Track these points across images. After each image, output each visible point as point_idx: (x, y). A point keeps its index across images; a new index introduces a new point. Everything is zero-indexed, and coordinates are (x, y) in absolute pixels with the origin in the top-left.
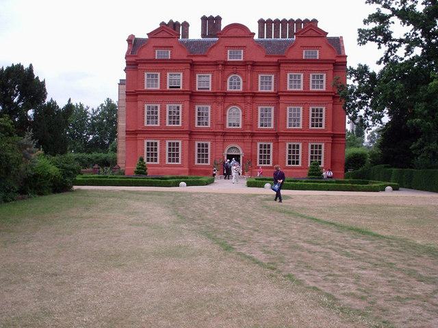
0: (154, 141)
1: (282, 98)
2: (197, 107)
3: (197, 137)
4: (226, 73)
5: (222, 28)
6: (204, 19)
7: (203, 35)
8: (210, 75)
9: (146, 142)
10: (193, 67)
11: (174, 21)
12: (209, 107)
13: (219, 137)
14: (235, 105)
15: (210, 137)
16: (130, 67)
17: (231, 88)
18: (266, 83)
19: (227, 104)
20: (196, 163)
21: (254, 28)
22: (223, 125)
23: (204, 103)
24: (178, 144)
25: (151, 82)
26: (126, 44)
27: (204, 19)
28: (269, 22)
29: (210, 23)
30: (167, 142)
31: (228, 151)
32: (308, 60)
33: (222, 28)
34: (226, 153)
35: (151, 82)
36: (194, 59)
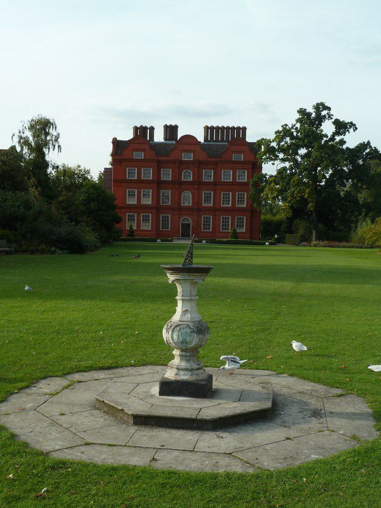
0: (133, 214)
1: (218, 187)
2: (161, 191)
5: (178, 138)
6: (166, 127)
7: (166, 139)
9: (127, 214)
10: (159, 165)
12: (170, 192)
14: (187, 190)
17: (184, 178)
18: (208, 176)
20: (161, 229)
21: (201, 138)
22: (180, 203)
23: (166, 189)
24: (149, 216)
25: (132, 174)
26: (111, 145)
27: (166, 127)
28: (212, 128)
29: (171, 130)
30: (142, 215)
32: (236, 161)
33: (178, 138)
35: (132, 174)
36: (160, 158)
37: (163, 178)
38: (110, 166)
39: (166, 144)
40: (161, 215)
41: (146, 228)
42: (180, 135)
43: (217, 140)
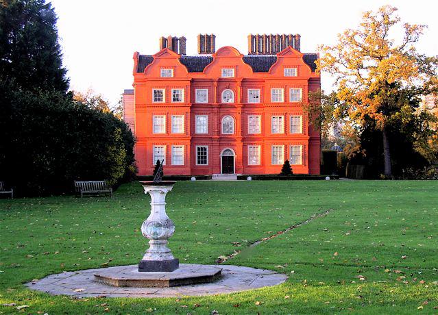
3: (196, 142)
4: (221, 88)
6: (201, 37)
7: (201, 52)
8: (207, 90)
11: (173, 36)
13: (216, 142)
15: (207, 142)
16: (138, 83)
19: (221, 114)
20: (197, 164)
22: (219, 132)
27: (201, 37)
28: (260, 37)
29: (206, 41)
31: (223, 154)
33: (216, 51)
34: (221, 155)
37: (198, 101)
38: (132, 88)
39: (201, 58)
40: (197, 147)
41: (178, 164)
42: (218, 45)
43: (266, 53)
